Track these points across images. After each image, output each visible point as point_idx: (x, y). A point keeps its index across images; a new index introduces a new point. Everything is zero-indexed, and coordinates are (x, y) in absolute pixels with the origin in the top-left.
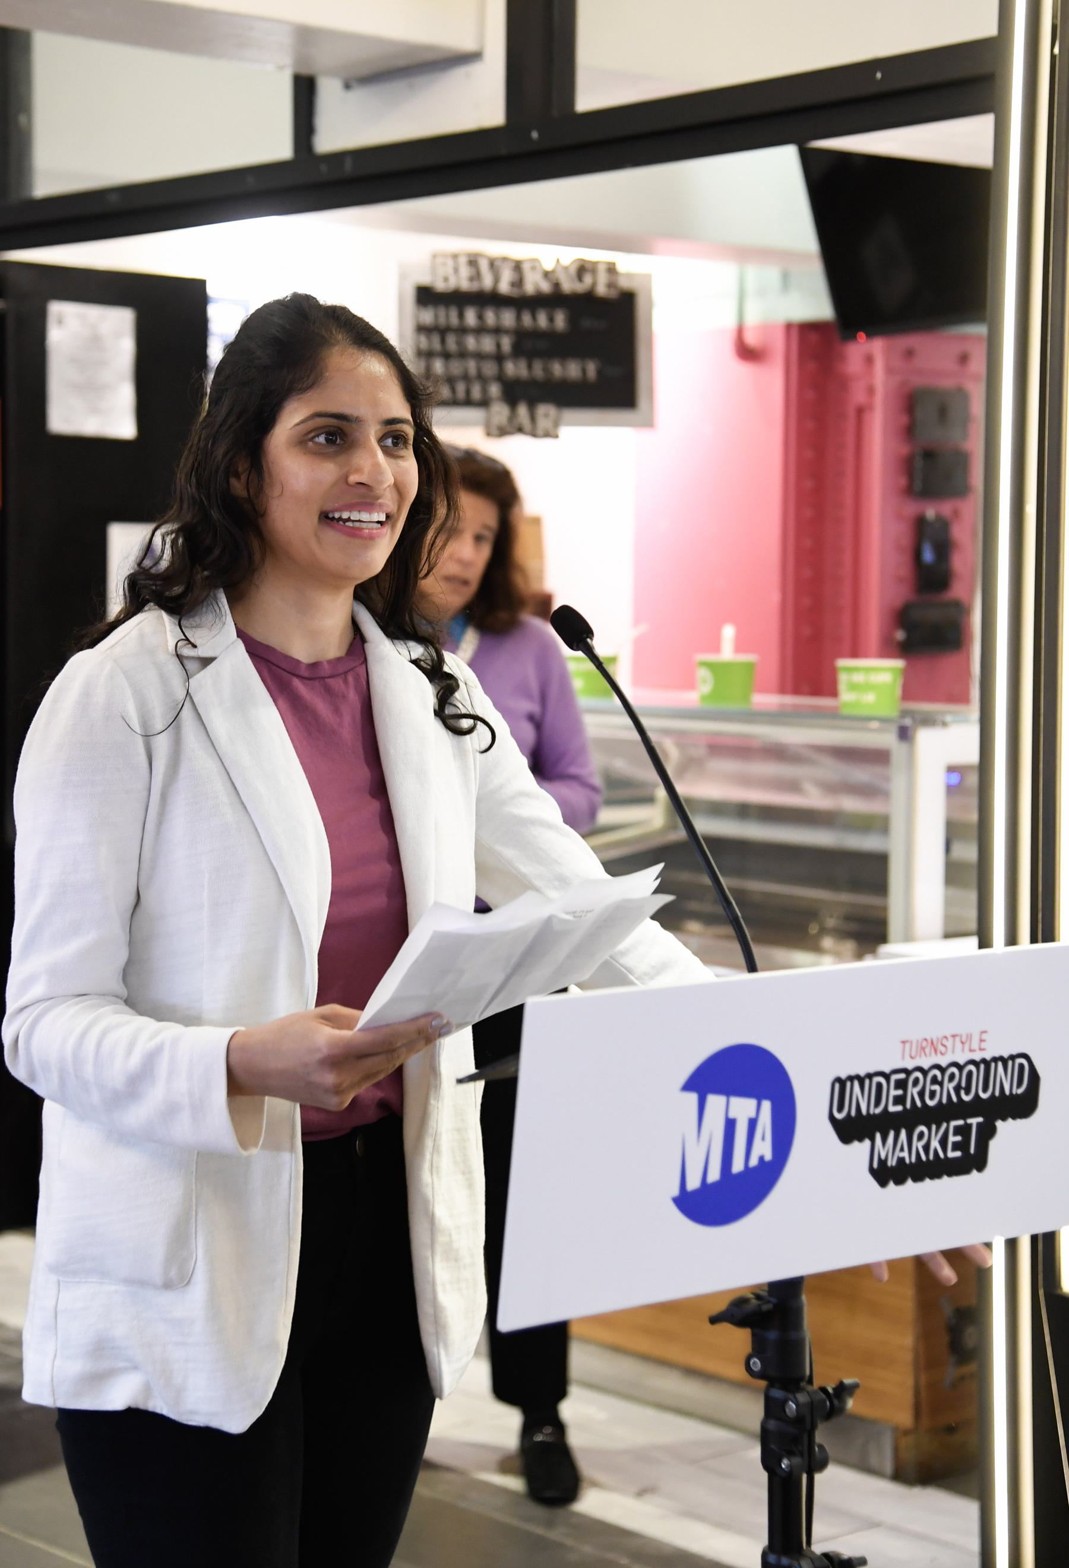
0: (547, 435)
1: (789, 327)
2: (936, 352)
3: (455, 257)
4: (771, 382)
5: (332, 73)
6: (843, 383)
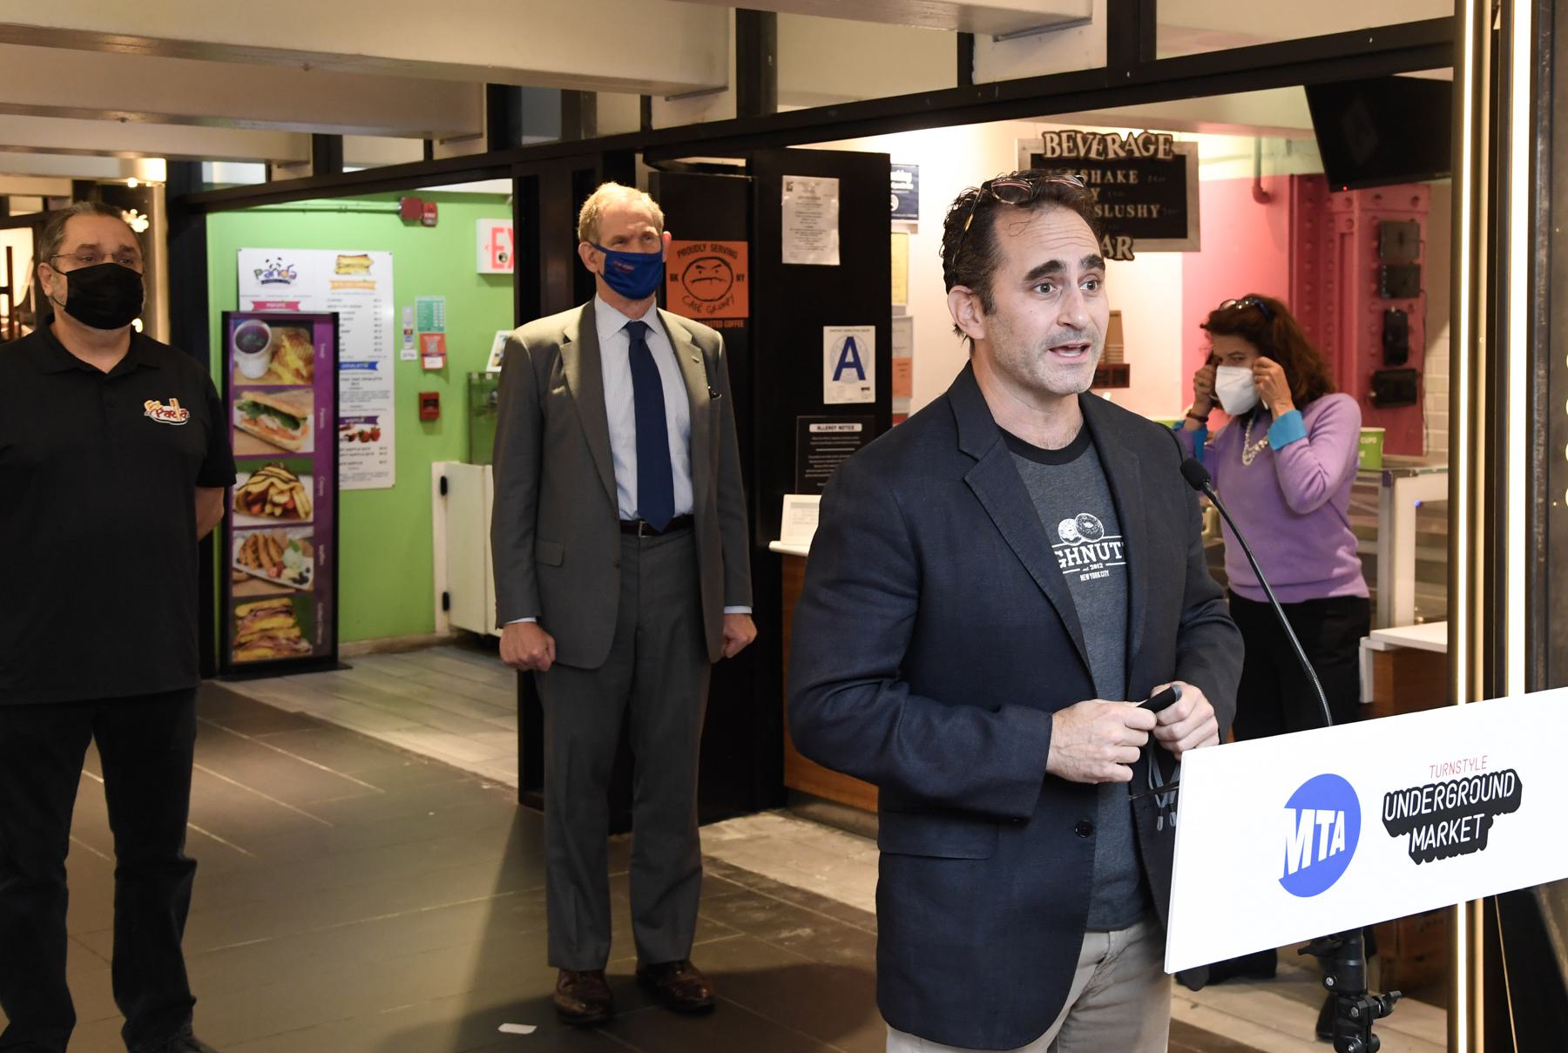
0: (1125, 258)
3: (1059, 134)
4: (1282, 214)
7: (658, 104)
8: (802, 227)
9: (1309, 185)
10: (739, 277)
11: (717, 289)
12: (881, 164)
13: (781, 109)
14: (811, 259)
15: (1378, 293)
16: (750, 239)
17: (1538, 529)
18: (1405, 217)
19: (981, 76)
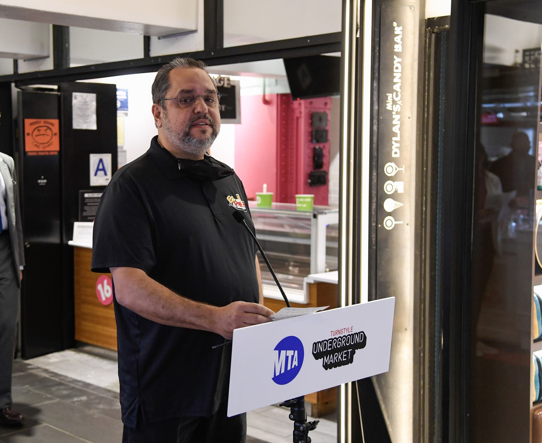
1: (278, 95)
2: (318, 103)
4: (273, 110)
5: (155, 35)
6: (293, 111)
7: (21, 63)
8: (81, 114)
9: (284, 98)
10: (55, 134)
11: (46, 139)
12: (112, 89)
13: (72, 65)
14: (84, 127)
15: (311, 141)
16: (59, 118)
17: (374, 236)
18: (322, 111)
19: (154, 53)
